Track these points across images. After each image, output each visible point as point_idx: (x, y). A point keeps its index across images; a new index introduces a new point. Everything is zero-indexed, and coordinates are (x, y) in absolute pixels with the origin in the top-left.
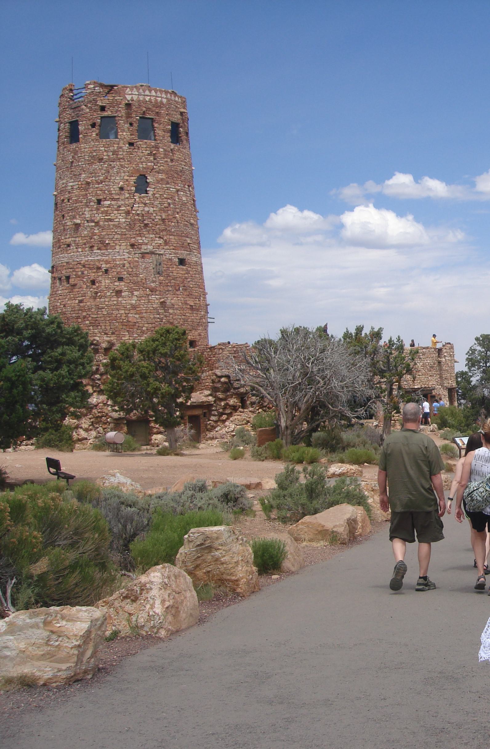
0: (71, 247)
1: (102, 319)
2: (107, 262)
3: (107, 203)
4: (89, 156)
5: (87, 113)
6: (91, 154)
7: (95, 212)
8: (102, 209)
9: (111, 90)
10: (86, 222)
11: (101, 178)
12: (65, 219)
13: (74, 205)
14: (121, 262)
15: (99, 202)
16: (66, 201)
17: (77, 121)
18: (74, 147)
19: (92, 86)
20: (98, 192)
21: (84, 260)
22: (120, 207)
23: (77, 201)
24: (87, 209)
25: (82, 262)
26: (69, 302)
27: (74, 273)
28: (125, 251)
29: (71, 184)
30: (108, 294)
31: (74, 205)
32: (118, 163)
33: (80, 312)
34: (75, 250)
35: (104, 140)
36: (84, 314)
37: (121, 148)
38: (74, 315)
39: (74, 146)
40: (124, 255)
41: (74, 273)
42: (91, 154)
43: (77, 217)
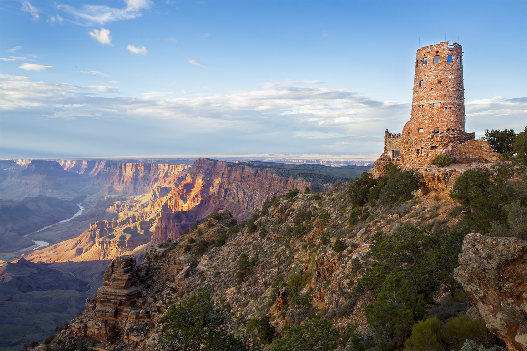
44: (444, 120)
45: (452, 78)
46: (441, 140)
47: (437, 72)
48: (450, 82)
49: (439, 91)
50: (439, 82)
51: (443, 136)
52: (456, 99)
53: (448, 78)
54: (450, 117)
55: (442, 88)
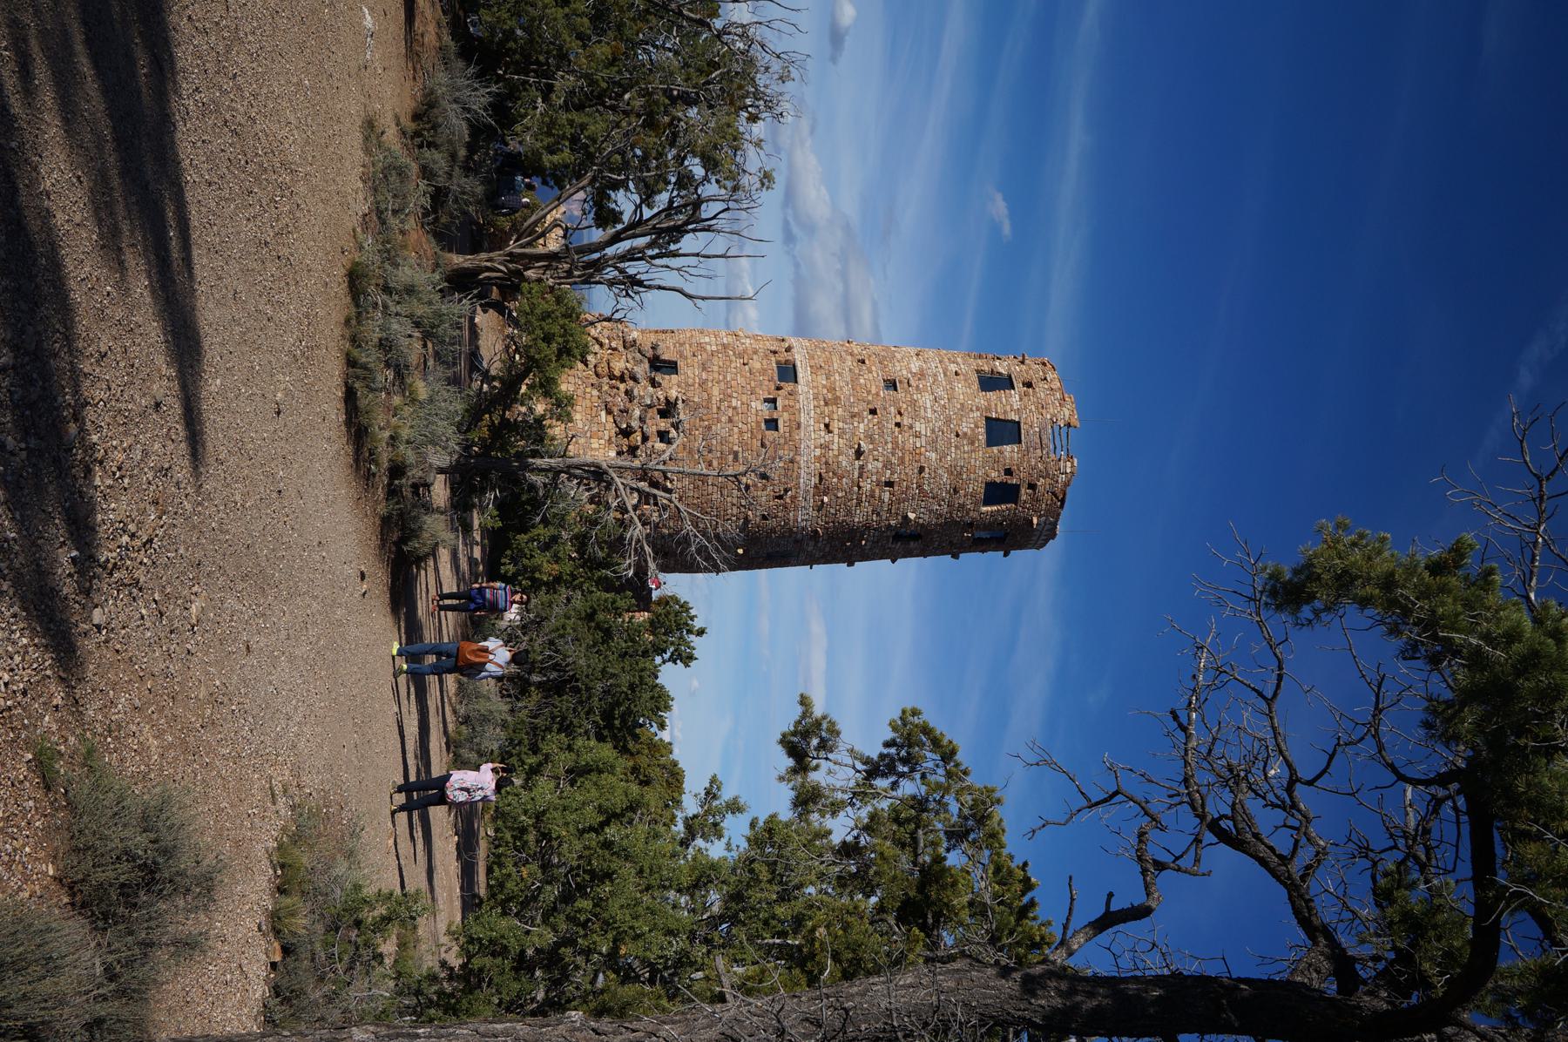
0: (823, 433)
1: (705, 493)
2: (794, 498)
3: (886, 497)
4: (962, 467)
5: (1029, 461)
6: (965, 470)
7: (874, 479)
8: (877, 491)
9: (1057, 498)
10: (861, 463)
11: (926, 487)
12: (870, 417)
13: (889, 439)
14: (792, 518)
15: (890, 484)
16: (898, 419)
17: (1020, 442)
18: (980, 437)
19: (1068, 471)
20: (905, 483)
21: (802, 460)
22: (878, 514)
23: (895, 443)
24: (880, 465)
25: (798, 458)
26: (736, 430)
27: (782, 441)
28: (809, 523)
29: (923, 432)
30: (743, 502)
31: (889, 439)
32: (945, 510)
33: (719, 454)
34: (819, 442)
35: (983, 491)
36: (715, 463)
37: (968, 514)
38: (714, 442)
39: (982, 438)
40: (802, 520)
41: (782, 441)
42: (965, 470)
43: (871, 447)
44: (715, 391)
45: (917, 435)
46: (617, 373)
47: (941, 377)
48: (898, 425)
49: (854, 380)
50: (892, 385)
51: (634, 379)
52: (818, 459)
53: (916, 417)
54: (730, 420)
55: (869, 392)
